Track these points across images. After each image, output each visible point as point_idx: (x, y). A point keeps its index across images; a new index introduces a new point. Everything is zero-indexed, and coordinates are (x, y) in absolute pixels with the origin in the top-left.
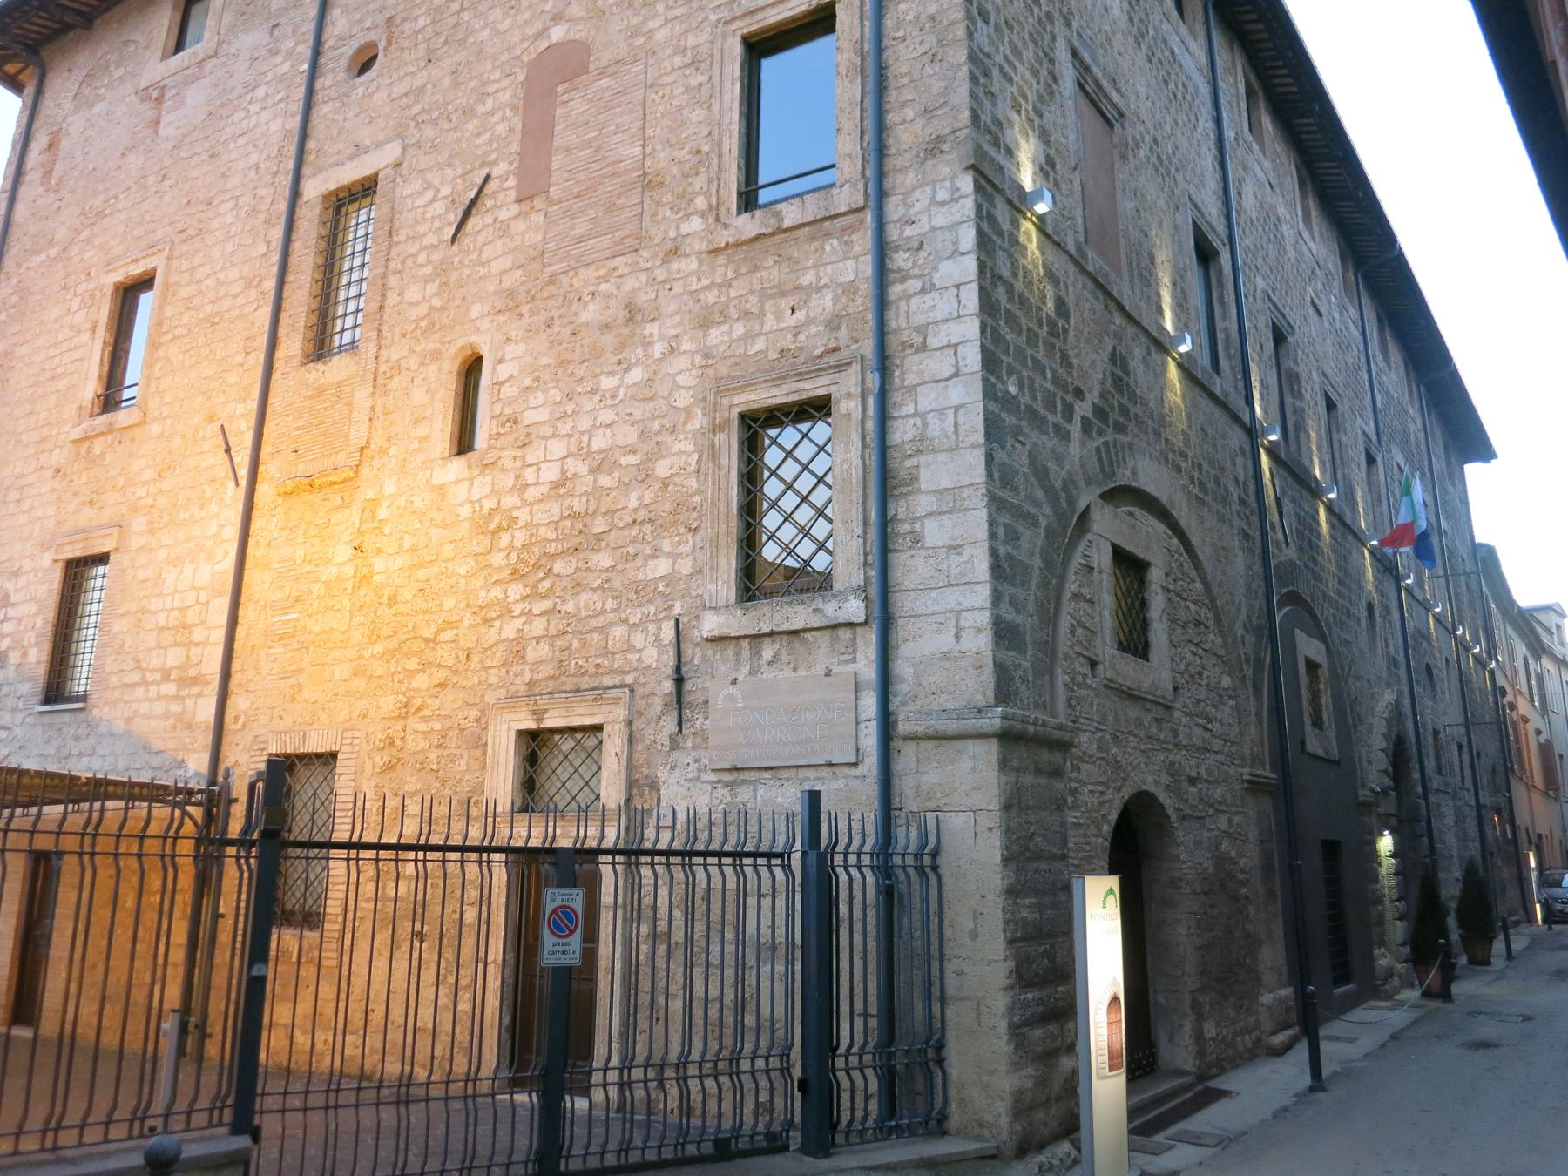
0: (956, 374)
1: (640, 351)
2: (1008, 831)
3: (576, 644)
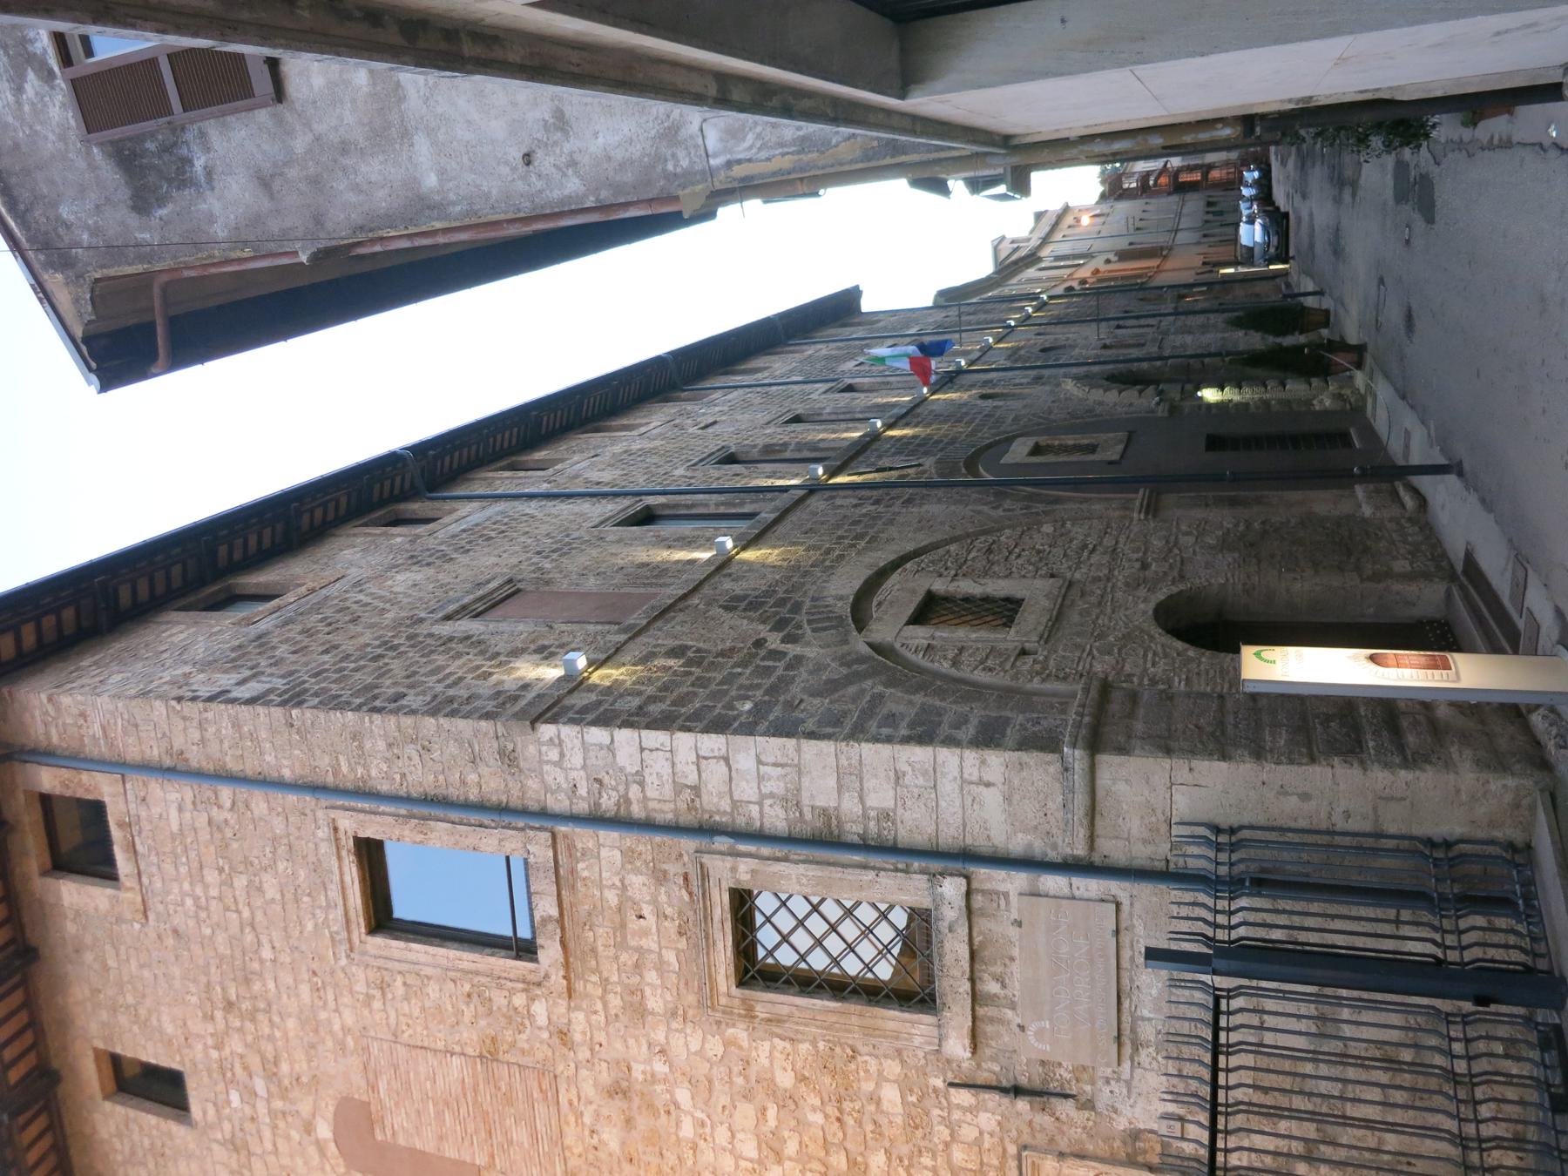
0: (726, 760)
1: (659, 1088)
2: (1192, 753)
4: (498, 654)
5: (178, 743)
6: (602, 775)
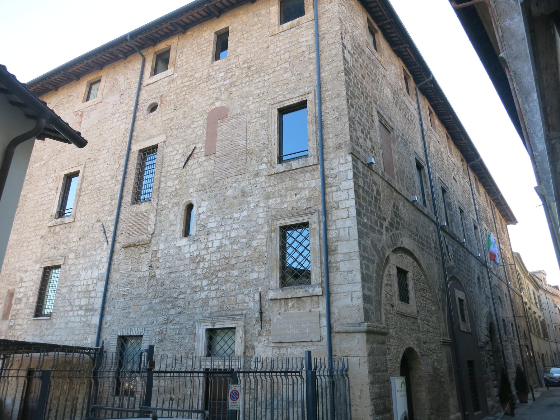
0: (348, 217)
1: (246, 205)
2: (370, 363)
4: (370, 134)
5: (327, 36)
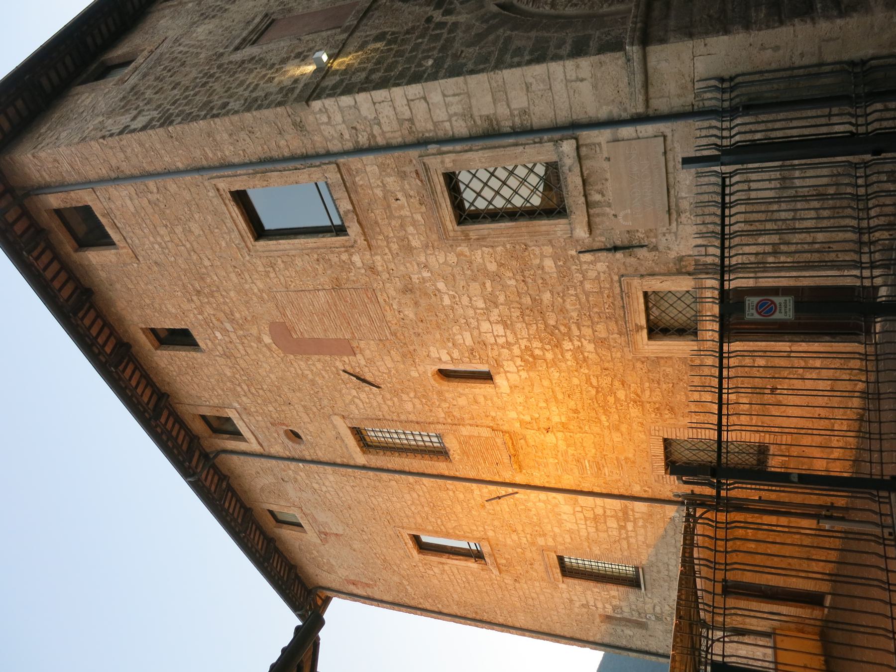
0: (425, 98)
1: (427, 285)
2: (707, 33)
3: (596, 310)
4: (274, 64)
6: (355, 124)
